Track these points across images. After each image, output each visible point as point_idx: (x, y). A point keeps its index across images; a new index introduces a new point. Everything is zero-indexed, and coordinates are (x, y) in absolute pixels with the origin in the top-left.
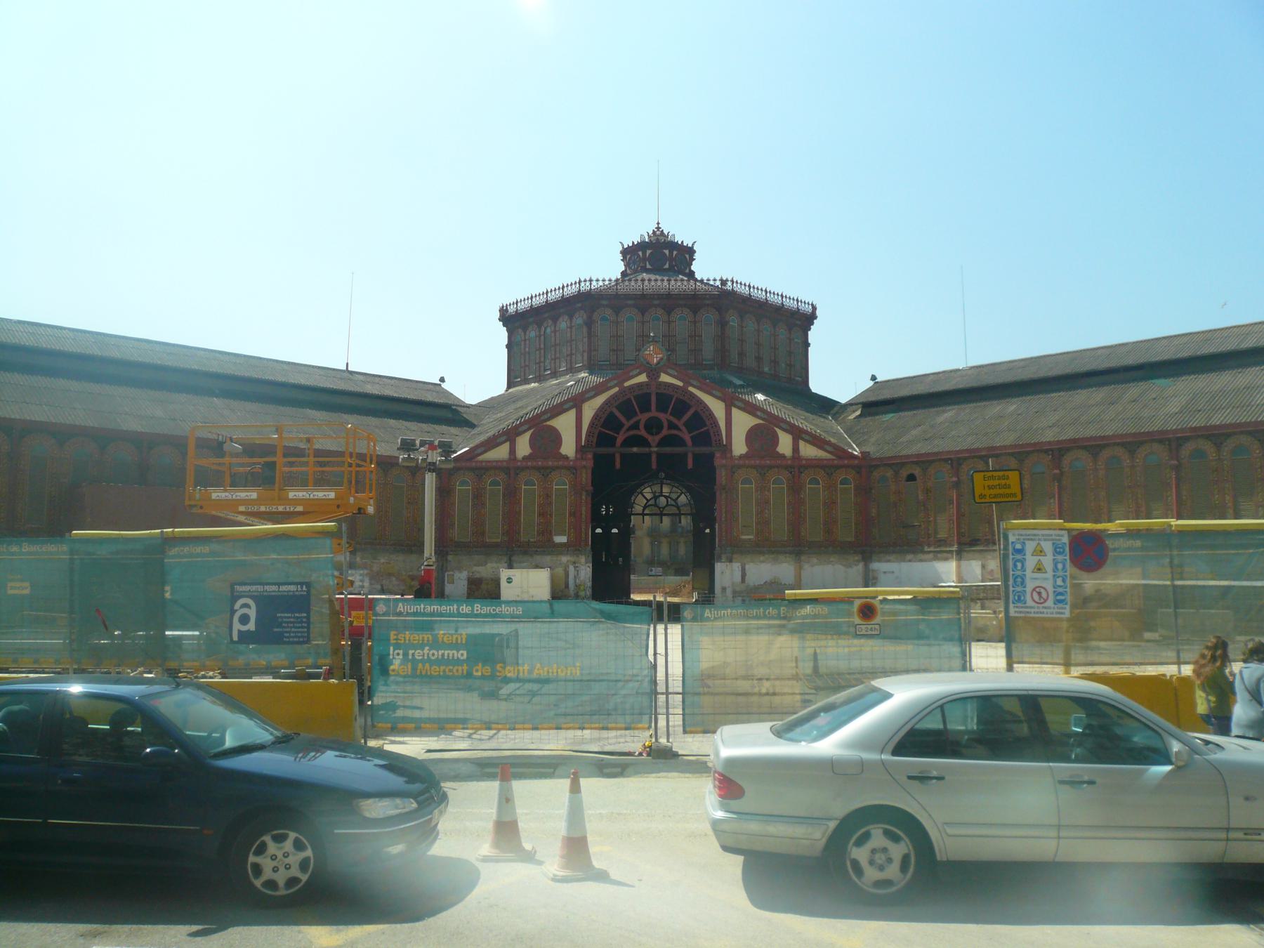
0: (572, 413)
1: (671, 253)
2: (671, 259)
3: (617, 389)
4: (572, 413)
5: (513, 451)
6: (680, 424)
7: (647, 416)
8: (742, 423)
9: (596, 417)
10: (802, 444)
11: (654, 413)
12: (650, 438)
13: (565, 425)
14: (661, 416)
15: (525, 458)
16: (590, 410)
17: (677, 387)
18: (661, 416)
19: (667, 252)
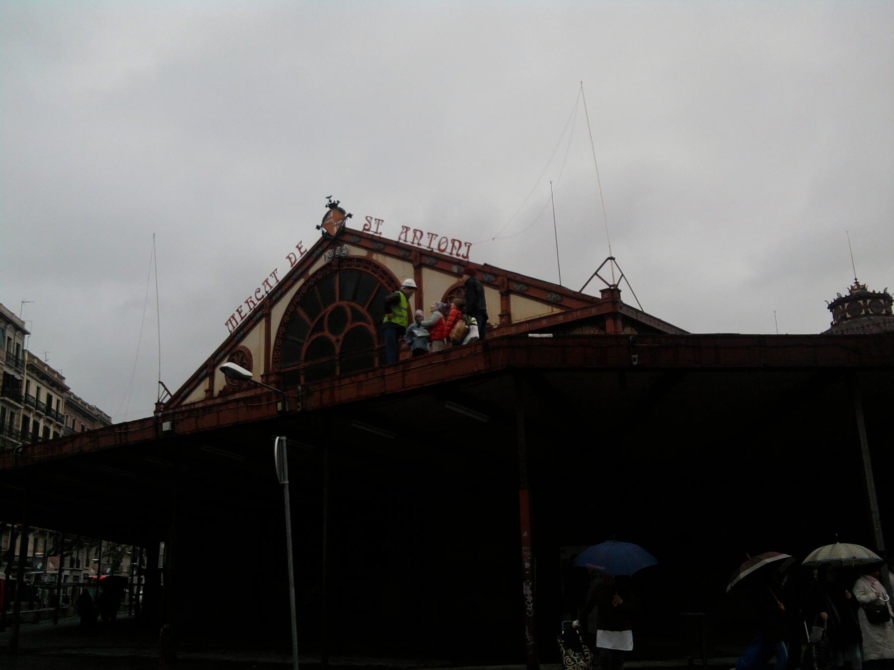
0: (263, 323)
1: (865, 302)
2: (866, 307)
3: (301, 282)
4: (263, 323)
5: (210, 390)
6: (363, 310)
7: (330, 308)
8: (437, 285)
9: (283, 324)
10: (515, 300)
11: (338, 302)
12: (333, 338)
13: (254, 342)
14: (344, 303)
15: (222, 393)
16: (278, 312)
17: (359, 260)
18: (344, 303)
19: (861, 302)
